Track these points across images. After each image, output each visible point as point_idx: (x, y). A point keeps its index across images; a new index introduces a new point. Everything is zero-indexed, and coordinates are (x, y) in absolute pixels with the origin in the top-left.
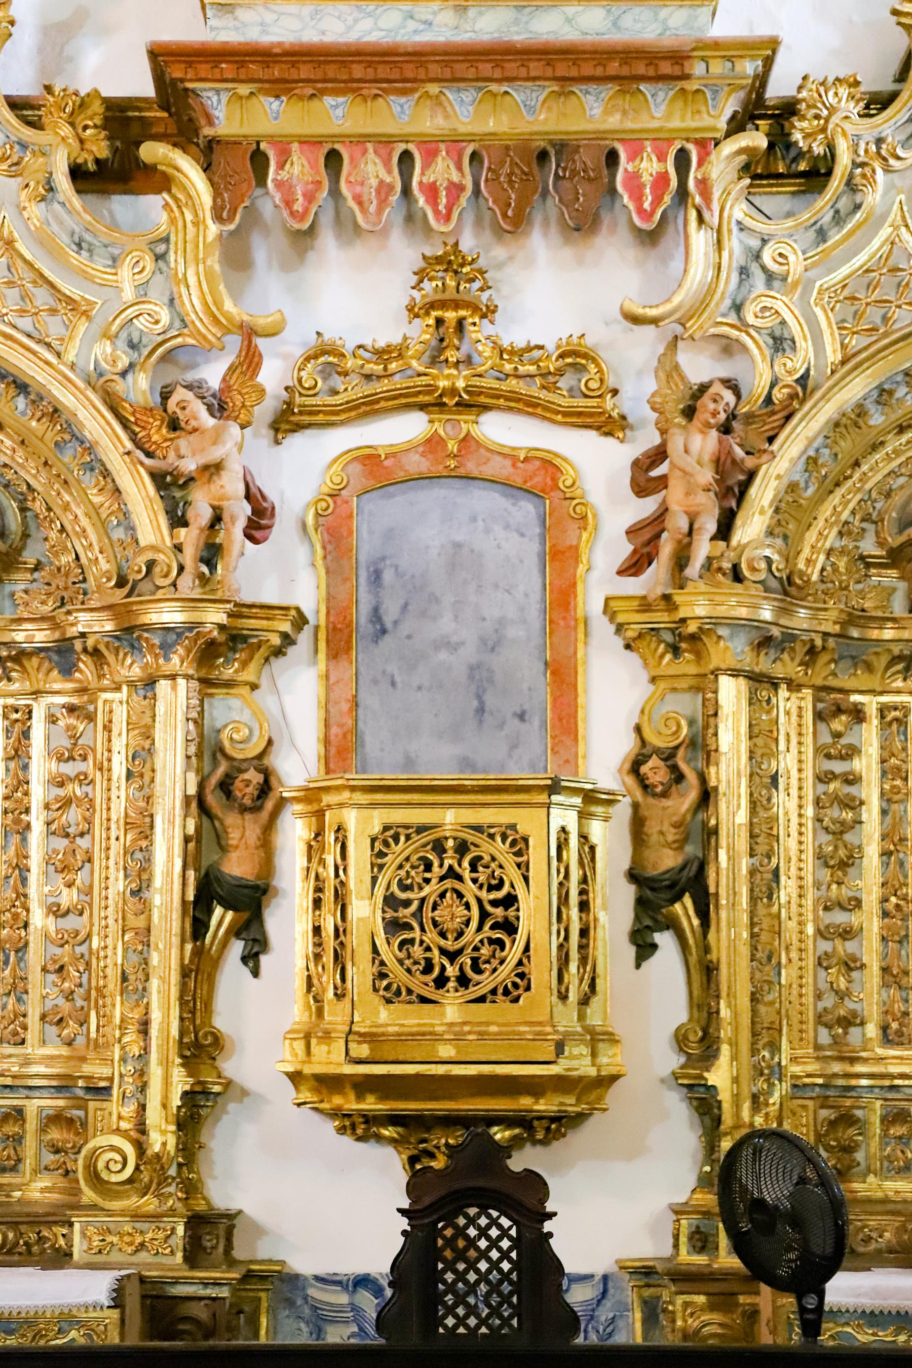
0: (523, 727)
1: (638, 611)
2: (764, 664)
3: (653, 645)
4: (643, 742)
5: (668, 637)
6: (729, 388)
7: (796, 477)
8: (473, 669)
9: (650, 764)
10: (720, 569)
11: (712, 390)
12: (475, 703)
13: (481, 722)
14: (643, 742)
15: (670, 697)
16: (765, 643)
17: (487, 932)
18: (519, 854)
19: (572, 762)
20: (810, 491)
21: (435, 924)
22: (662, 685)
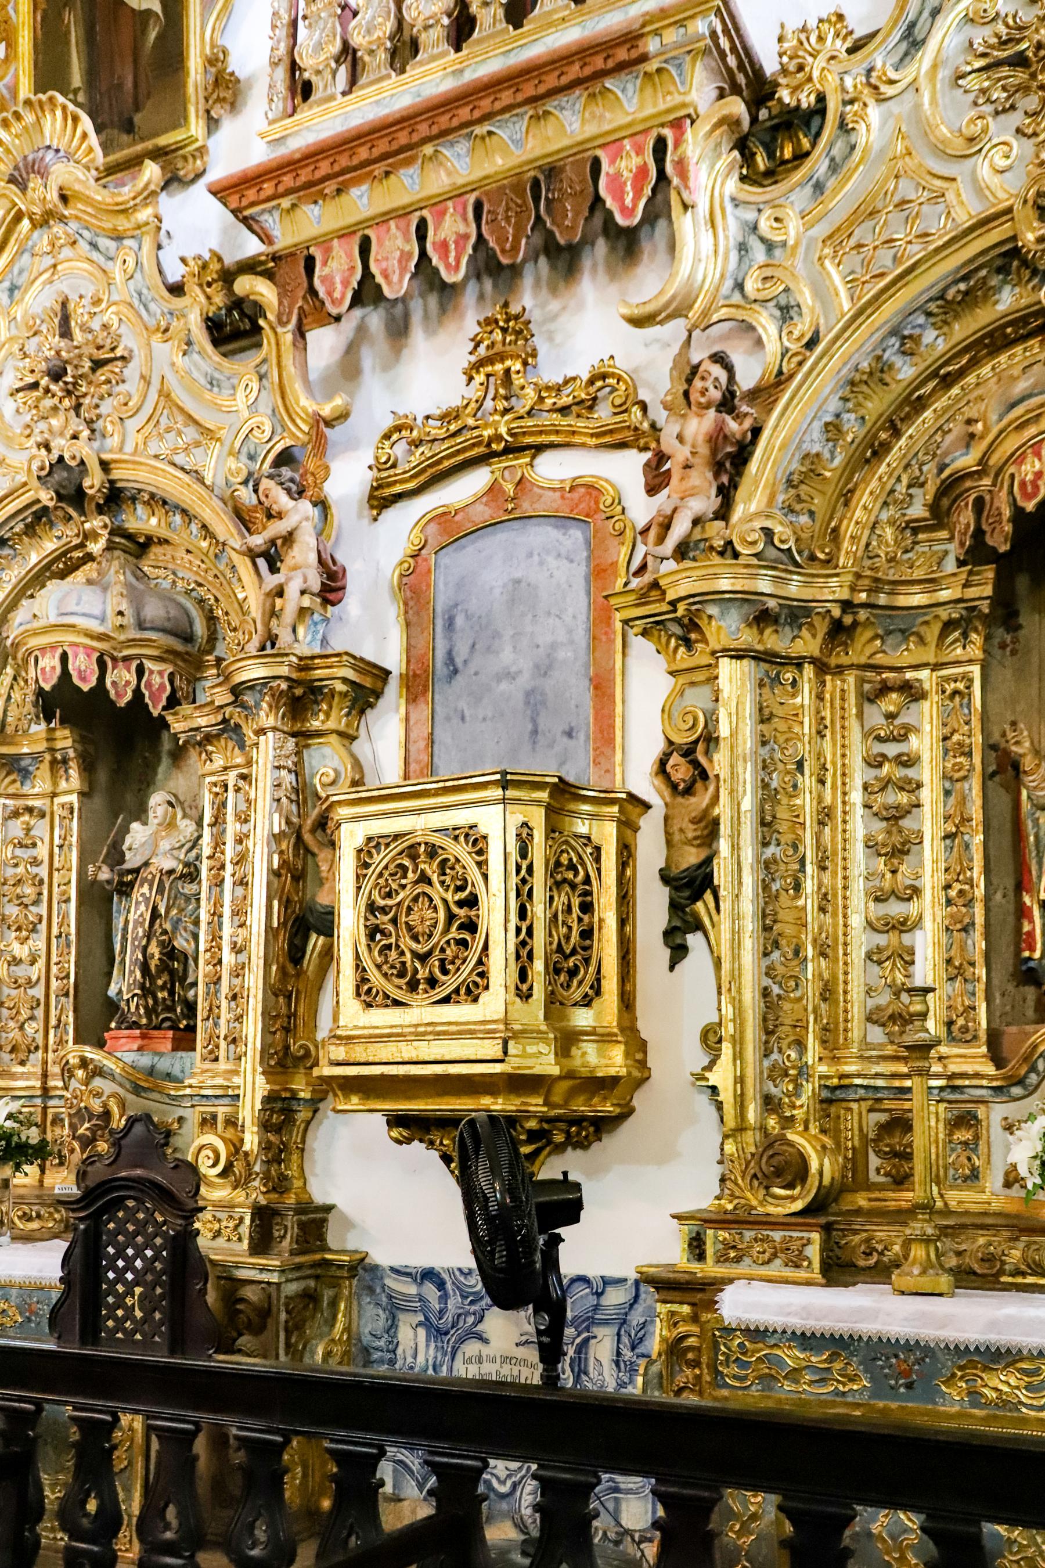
0: (571, 743)
1: (637, 605)
2: (774, 641)
3: (664, 640)
4: (670, 743)
5: (677, 630)
6: (716, 362)
7: (816, 448)
8: (529, 694)
9: (671, 762)
10: (712, 548)
11: (701, 369)
12: (530, 727)
13: (534, 743)
14: (670, 743)
15: (689, 692)
16: (763, 619)
17: (454, 933)
18: (480, 852)
19: (610, 771)
20: (837, 462)
21: (410, 928)
22: (682, 680)
